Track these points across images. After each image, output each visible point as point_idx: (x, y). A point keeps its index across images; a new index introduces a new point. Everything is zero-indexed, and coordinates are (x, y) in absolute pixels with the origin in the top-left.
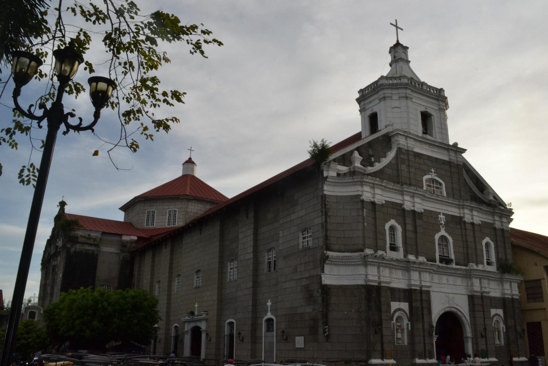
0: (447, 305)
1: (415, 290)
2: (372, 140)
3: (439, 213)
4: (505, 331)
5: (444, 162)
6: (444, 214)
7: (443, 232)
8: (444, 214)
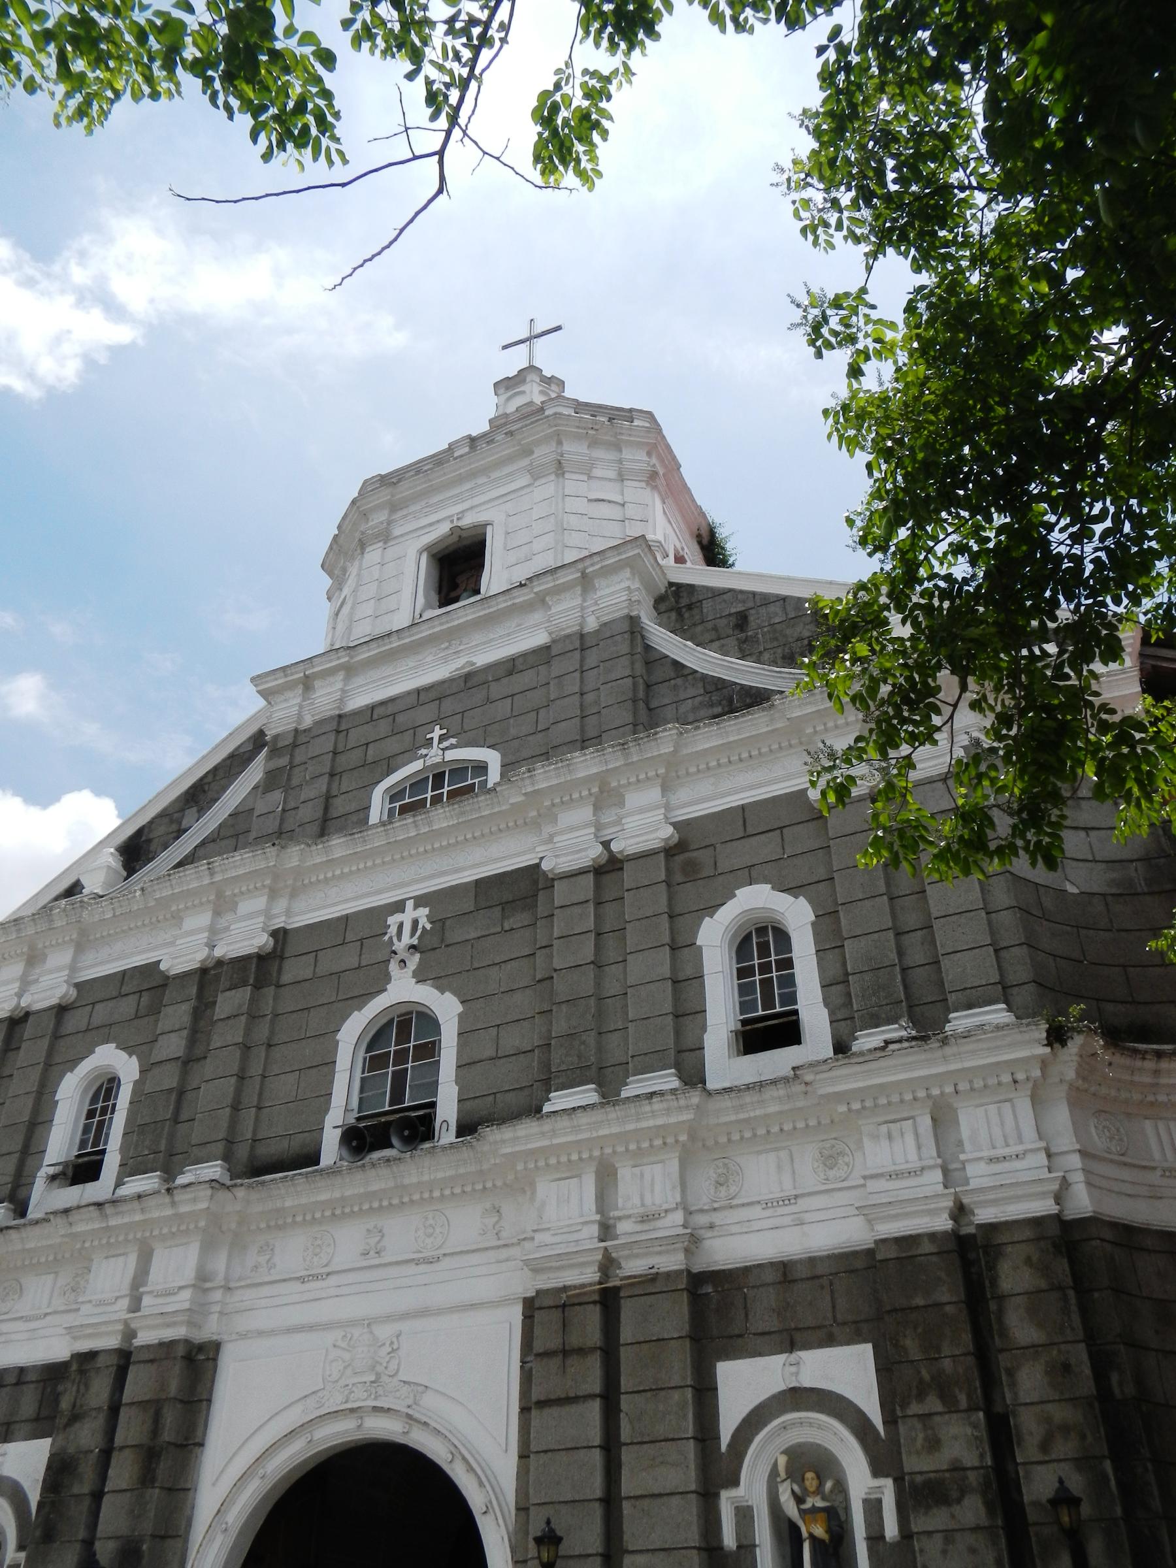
0: (334, 1402)
1: (92, 1355)
2: (201, 779)
3: (399, 907)
4: (891, 1529)
5: (511, 666)
6: (420, 901)
7: (404, 988)
8: (420, 901)
